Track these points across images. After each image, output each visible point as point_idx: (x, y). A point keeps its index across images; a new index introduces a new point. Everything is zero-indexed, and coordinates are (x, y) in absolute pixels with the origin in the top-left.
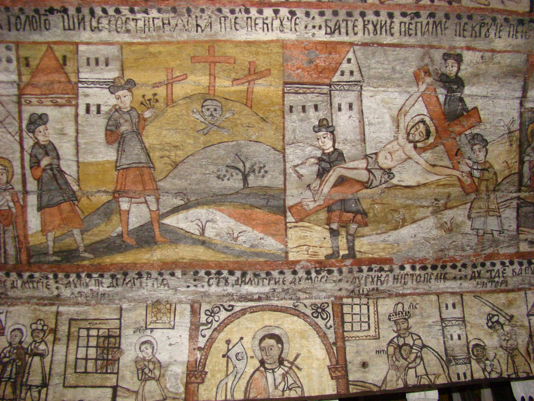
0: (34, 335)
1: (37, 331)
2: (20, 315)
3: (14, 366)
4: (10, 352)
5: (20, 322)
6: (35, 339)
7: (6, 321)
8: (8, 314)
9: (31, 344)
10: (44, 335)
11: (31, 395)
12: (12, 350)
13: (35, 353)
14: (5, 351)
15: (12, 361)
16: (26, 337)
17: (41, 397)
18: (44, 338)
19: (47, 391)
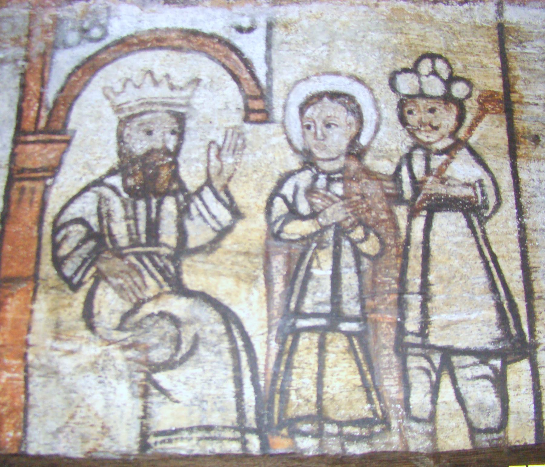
0: (412, 120)
1: (421, 102)
2: (333, 37)
3: (347, 258)
4: (311, 191)
5: (337, 65)
6: (422, 136)
7: (268, 60)
8: (279, 34)
9: (408, 157)
10: (461, 119)
11: (460, 399)
12: (322, 181)
13: (438, 197)
14: (288, 190)
15: (330, 235)
16: (377, 129)
17: (513, 404)
18: (462, 134)
19: (535, 375)
